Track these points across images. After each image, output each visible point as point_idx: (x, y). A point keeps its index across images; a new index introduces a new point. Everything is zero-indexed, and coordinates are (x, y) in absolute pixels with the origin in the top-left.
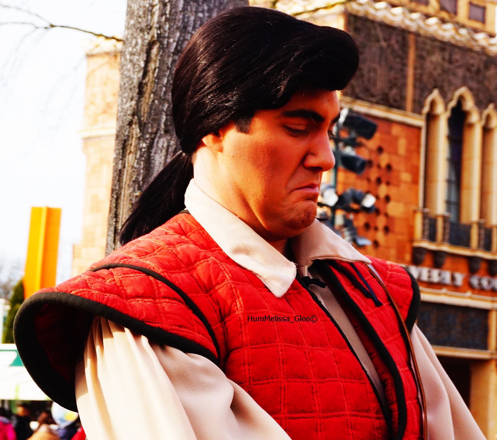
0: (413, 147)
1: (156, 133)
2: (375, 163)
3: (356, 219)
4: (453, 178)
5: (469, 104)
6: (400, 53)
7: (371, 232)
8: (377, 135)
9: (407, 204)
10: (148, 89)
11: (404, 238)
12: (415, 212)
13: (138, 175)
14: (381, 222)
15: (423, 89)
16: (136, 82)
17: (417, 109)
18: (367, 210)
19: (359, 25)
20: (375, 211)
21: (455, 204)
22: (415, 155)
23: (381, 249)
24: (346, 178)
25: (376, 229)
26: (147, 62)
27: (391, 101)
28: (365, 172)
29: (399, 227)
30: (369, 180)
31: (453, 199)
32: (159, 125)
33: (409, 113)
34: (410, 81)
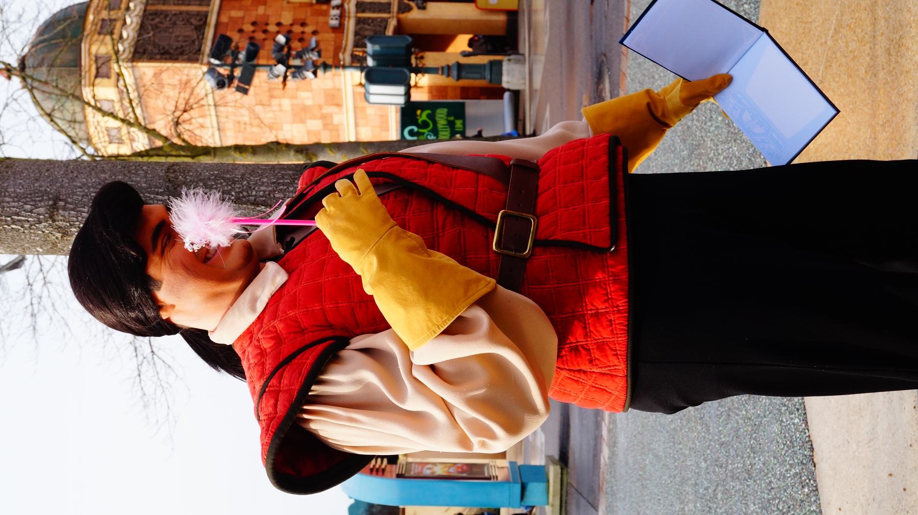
2: (251, 35)
3: (295, 49)
6: (162, 16)
7: (305, 36)
8: (229, 34)
9: (283, 9)
11: (309, 10)
14: (297, 29)
19: (141, 50)
20: (289, 34)
23: (319, 29)
24: (263, 57)
25: (303, 33)
27: (201, 23)
28: (258, 43)
29: (301, 15)
30: (265, 39)
33: (210, 8)
34: (184, 8)
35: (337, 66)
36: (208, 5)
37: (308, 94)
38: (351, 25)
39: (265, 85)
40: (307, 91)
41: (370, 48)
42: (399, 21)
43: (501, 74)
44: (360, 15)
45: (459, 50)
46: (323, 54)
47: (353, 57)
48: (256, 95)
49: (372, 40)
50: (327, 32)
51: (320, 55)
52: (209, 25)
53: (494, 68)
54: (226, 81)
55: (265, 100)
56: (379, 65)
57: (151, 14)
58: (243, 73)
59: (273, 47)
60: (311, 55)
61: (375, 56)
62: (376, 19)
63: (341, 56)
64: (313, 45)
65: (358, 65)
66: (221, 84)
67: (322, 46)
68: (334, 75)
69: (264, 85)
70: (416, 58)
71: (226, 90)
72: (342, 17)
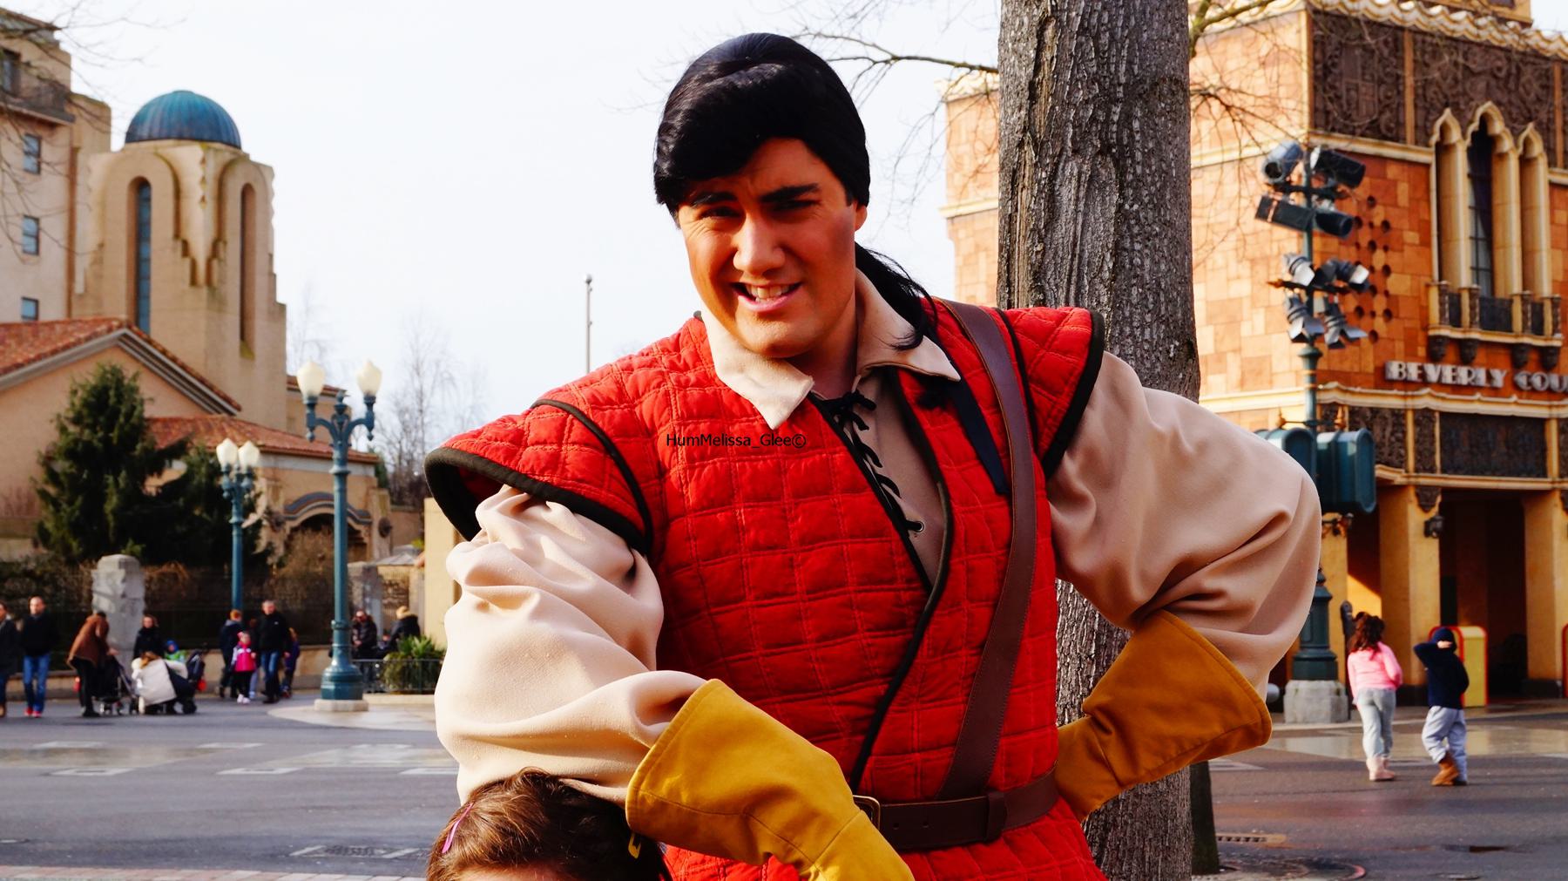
0: (1419, 194)
1: (1060, 155)
2: (1365, 221)
3: (1342, 302)
4: (1481, 234)
5: (1498, 127)
7: (1366, 320)
8: (1366, 180)
9: (1415, 275)
10: (1043, 92)
11: (1416, 324)
12: (1428, 286)
13: (1038, 220)
14: (1379, 304)
15: (1428, 111)
16: (1024, 81)
17: (1422, 137)
18: (1358, 288)
20: (1368, 289)
21: (1487, 269)
22: (1423, 204)
23: (1381, 343)
24: (1325, 245)
25: (1373, 314)
26: (1039, 50)
27: (1384, 131)
29: (1405, 310)
30: (1358, 245)
31: (1482, 264)
32: (1064, 142)
34: (1409, 99)
35: (1314, 379)
36: (1416, 143)
37: (1260, 329)
38: (1390, 401)
39: (1275, 251)
40: (1267, 324)
41: (1351, 437)
42: (1402, 488)
43: (1312, 677)
44: (1410, 416)
45: (1351, 599)
46: (1336, 352)
47: (1333, 407)
48: (1255, 233)
49: (1365, 441)
50: (1376, 357)
51: (1333, 346)
52: (1352, 141)
53: (1322, 664)
54: (1280, 179)
55: (1252, 251)
56: (1319, 453)
57: (1396, 40)
58: (1296, 208)
59: (1345, 261)
60: (1332, 331)
61: (1335, 445)
62: (1406, 449)
63: (1334, 384)
64: (1352, 334)
65: (1318, 417)
66: (1271, 170)
67: (1350, 349)
68: (1297, 372)
69: (1275, 246)
70: (1334, 522)
71: (1262, 177)
72: (1405, 384)
